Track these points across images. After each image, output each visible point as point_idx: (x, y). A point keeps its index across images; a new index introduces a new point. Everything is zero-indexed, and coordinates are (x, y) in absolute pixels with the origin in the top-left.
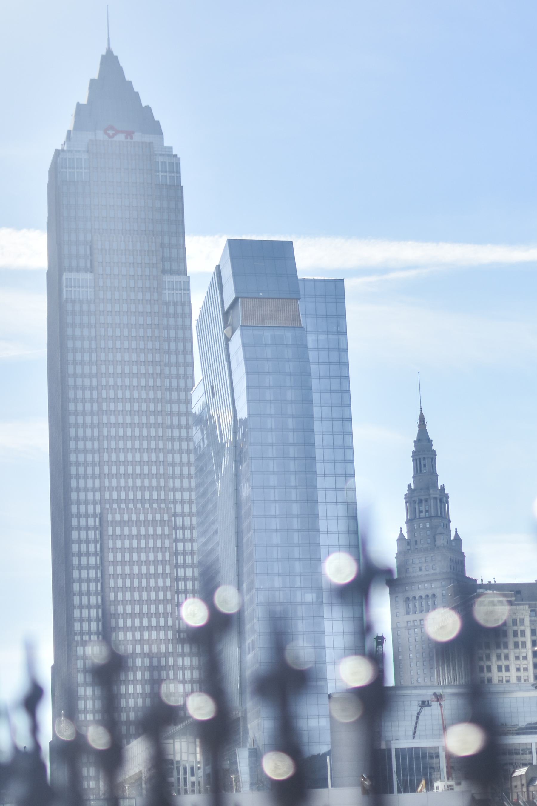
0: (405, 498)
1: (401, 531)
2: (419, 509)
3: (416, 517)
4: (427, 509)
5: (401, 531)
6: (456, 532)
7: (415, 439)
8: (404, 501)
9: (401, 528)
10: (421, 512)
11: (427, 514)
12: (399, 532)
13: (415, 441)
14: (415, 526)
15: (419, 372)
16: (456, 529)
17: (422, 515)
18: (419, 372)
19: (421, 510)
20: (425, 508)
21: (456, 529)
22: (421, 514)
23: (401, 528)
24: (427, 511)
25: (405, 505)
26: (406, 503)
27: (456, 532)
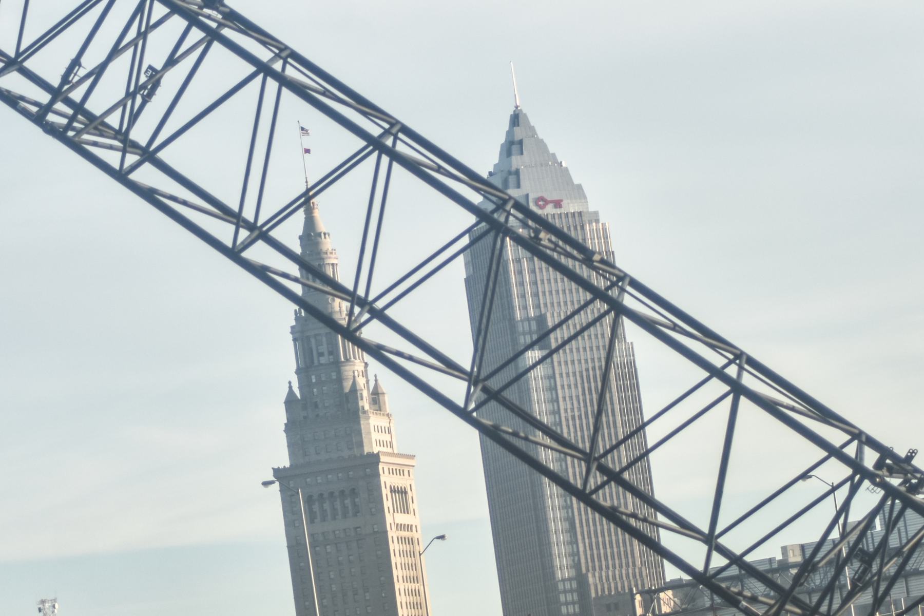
0: (292, 333)
1: (290, 387)
2: (317, 350)
3: (312, 362)
4: (330, 349)
5: (290, 387)
6: (376, 380)
7: (301, 234)
8: (291, 337)
9: (290, 383)
10: (321, 354)
11: (331, 357)
12: (287, 390)
13: (300, 238)
14: (313, 377)
15: (298, 122)
16: (376, 376)
17: (323, 360)
18: (298, 122)
19: (320, 351)
20: (328, 348)
21: (376, 376)
22: (321, 358)
23: (290, 383)
24: (331, 353)
25: (292, 343)
26: (295, 340)
27: (376, 380)
